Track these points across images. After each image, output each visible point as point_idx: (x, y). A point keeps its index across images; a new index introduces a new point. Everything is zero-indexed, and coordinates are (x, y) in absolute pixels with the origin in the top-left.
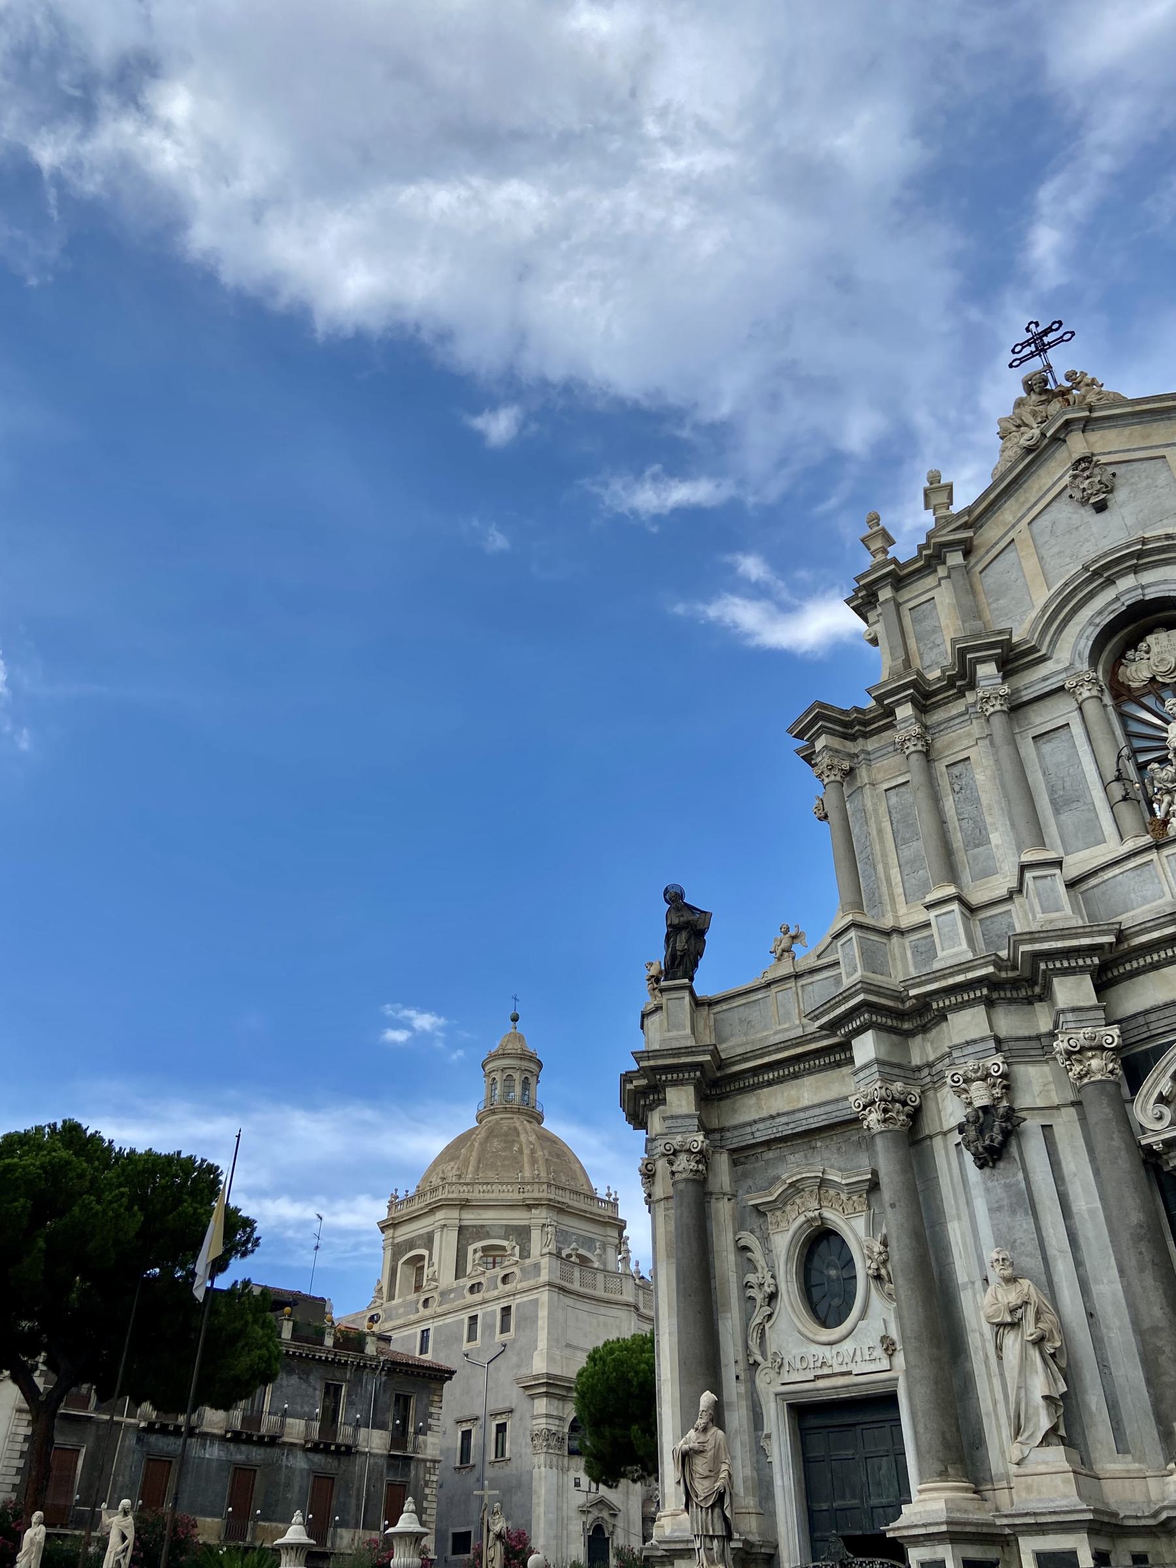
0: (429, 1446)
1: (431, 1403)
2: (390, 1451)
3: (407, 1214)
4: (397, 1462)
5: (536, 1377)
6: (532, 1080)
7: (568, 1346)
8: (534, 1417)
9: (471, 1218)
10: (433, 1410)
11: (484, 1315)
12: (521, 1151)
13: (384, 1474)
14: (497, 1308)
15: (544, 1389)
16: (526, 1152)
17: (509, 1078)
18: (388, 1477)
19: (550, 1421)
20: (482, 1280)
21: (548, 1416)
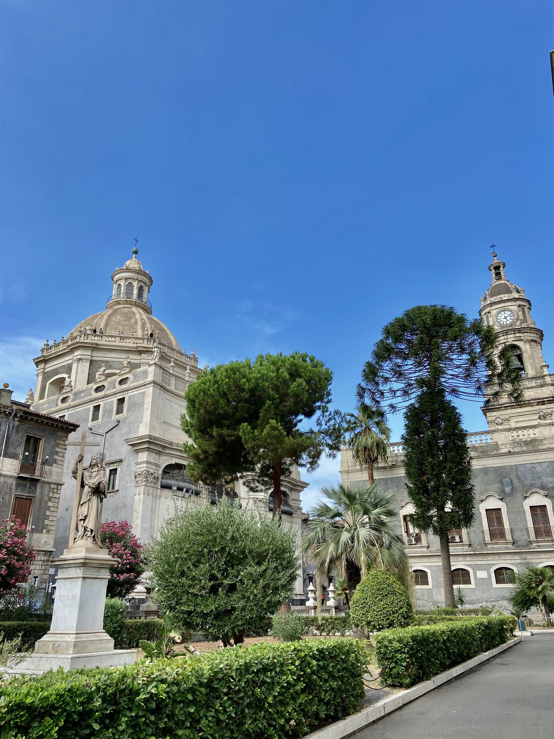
0: (54, 473)
1: (58, 445)
2: (19, 474)
3: (55, 353)
4: (25, 483)
5: (141, 437)
6: (146, 289)
7: (164, 422)
8: (137, 464)
9: (99, 356)
10: (58, 450)
11: (105, 405)
12: (136, 322)
13: (13, 491)
14: (115, 399)
15: (146, 446)
16: (139, 323)
17: (130, 285)
18: (16, 491)
19: (150, 466)
20: (104, 383)
21: (148, 462)
